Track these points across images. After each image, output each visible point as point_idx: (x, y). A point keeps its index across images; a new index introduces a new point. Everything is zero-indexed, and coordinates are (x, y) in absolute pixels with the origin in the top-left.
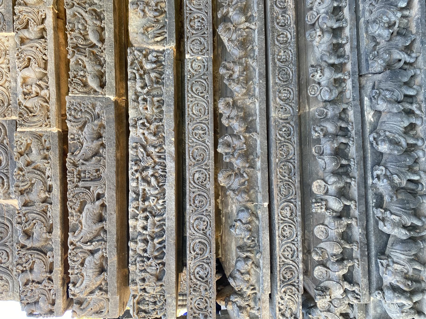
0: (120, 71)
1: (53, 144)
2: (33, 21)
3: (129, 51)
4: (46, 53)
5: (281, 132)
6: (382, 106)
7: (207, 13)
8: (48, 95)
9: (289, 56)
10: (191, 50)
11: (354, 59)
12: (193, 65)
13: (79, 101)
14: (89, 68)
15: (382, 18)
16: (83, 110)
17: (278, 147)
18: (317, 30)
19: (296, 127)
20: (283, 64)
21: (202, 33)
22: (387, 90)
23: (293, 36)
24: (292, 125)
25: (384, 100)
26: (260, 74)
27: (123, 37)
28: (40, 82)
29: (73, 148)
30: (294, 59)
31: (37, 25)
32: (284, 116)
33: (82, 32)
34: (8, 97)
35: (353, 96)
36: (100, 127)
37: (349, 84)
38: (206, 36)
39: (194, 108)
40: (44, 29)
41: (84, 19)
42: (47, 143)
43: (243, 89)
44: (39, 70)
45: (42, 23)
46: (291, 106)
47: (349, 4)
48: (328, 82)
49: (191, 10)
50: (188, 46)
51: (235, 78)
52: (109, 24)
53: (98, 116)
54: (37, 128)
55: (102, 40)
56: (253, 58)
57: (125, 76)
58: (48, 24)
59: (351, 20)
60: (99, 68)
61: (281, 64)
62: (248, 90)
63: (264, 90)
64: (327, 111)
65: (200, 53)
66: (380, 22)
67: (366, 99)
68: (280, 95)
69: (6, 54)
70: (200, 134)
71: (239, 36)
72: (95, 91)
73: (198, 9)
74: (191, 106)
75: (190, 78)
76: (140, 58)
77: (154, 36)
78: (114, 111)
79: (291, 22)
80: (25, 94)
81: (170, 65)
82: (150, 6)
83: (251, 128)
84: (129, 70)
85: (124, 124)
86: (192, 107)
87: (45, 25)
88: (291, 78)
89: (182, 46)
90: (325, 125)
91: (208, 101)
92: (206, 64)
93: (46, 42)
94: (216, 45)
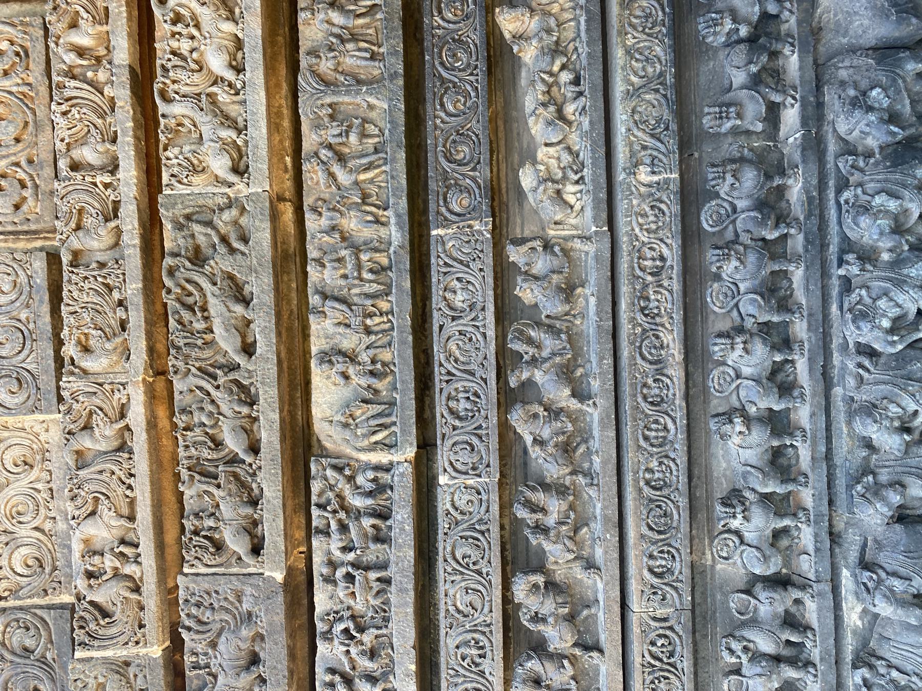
0: (293, 492)
1: (151, 684)
2: (102, 415)
4: (133, 485)
5: (654, 649)
6: (884, 609)
7: (485, 381)
8: (139, 574)
9: (671, 473)
10: (451, 463)
11: (820, 484)
12: (456, 498)
13: (206, 586)
14: (227, 511)
15: (886, 409)
16: (216, 605)
17: (648, 682)
18: (736, 420)
19: (687, 637)
20: (658, 493)
22: (895, 574)
23: (681, 427)
24: (677, 633)
25: (888, 598)
26: (606, 519)
27: (300, 413)
28: (122, 549)
29: (195, 682)
30: (683, 479)
31: (112, 422)
32: (661, 612)
33: (210, 431)
35: (817, 571)
36: (253, 640)
37: (806, 536)
38: (484, 432)
39: (458, 596)
40: (128, 428)
41: (213, 402)
42: (140, 680)
43: (567, 554)
44: (119, 523)
45: (123, 416)
46: (676, 589)
47: (809, 359)
48: (760, 536)
49: (449, 373)
50: (443, 456)
51: (548, 525)
52: (269, 413)
53: (250, 614)
54: (118, 649)
55: (254, 449)
56: (587, 474)
57: (303, 499)
59: (814, 395)
60: (249, 511)
61: (653, 492)
62: (580, 545)
63: (616, 555)
64: (757, 602)
65: (470, 472)
66: (881, 419)
67: (845, 573)
68: (651, 563)
69: (44, 460)
70: (472, 656)
71: (557, 434)
72: (240, 558)
73: (465, 371)
74: (451, 592)
75: (449, 528)
76: (340, 486)
77: (369, 431)
78: (283, 607)
79: (674, 395)
80: (90, 575)
81: (405, 501)
82: (360, 364)
83: (587, 631)
84: (315, 512)
85: (304, 609)
86: (454, 596)
87: (127, 420)
88: (675, 525)
89: (427, 407)
90: (752, 638)
91: (490, 582)
92: (484, 497)
93: (130, 458)
94: (502, 400)
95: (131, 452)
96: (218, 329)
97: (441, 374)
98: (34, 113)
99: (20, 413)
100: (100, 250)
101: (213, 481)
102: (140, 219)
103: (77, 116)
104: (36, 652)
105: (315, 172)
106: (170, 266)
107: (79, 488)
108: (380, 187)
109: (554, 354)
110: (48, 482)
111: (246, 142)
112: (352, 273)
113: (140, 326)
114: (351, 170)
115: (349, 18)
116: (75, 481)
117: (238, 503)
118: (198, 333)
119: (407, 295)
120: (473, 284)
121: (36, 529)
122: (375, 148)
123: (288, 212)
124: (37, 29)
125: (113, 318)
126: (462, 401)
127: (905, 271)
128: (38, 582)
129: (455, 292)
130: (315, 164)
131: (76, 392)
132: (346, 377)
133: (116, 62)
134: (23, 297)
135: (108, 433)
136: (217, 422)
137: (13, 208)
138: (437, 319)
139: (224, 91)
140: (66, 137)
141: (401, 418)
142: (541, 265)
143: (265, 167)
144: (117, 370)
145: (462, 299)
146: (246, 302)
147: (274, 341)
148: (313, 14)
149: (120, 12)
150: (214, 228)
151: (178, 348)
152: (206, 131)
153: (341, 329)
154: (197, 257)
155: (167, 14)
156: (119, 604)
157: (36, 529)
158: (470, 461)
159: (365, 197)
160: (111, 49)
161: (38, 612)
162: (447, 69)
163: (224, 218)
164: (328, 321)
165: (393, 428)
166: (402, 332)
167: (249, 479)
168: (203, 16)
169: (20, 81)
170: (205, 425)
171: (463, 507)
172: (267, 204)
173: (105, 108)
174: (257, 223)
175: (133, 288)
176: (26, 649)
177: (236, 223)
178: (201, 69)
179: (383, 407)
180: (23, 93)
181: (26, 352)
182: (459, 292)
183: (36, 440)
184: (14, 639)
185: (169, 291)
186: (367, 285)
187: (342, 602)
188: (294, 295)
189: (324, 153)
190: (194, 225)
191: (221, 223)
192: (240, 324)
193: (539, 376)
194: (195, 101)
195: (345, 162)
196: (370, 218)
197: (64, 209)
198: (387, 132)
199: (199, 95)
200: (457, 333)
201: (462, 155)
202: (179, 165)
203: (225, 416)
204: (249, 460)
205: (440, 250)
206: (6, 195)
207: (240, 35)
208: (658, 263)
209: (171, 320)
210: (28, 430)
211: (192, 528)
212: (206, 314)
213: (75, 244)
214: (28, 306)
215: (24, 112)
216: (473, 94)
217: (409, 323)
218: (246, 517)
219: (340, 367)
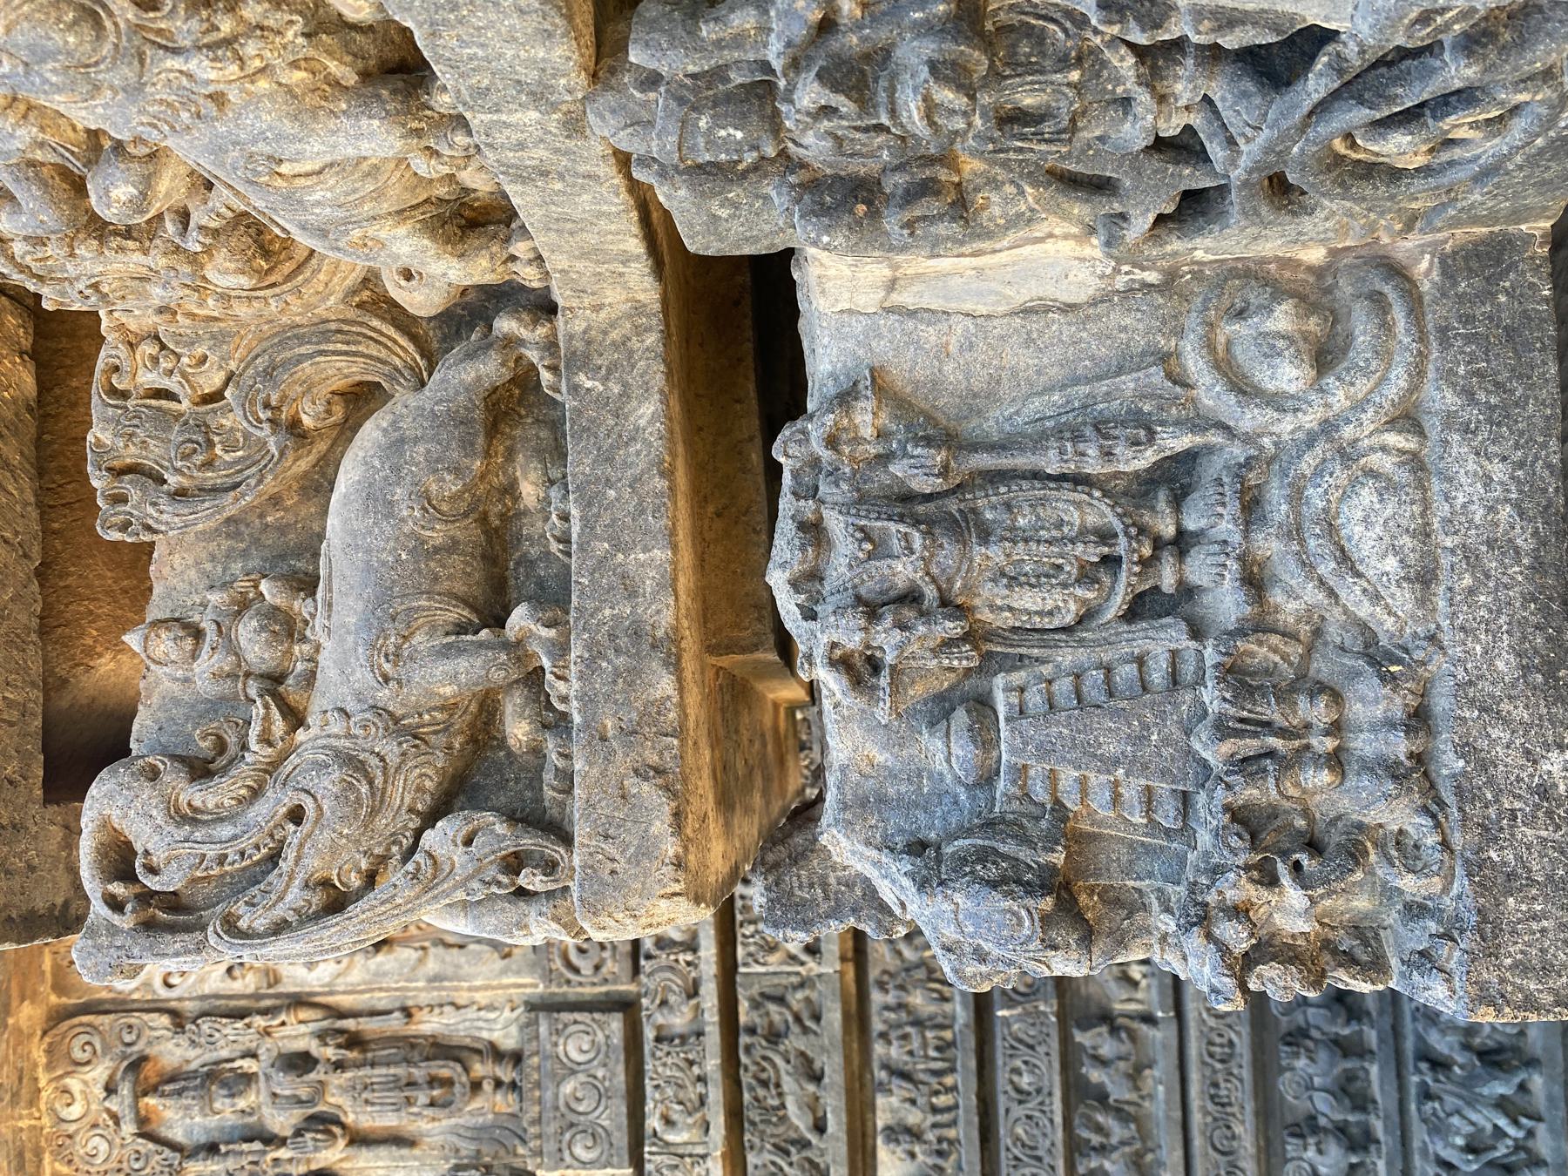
49: (1016, 1158)
96: (792, 1108)
109: (1123, 1143)
125: (693, 1092)
127: (1477, 1090)
132: (912, 1155)
134: (601, 1056)
138: (1002, 1102)
142: (1107, 1048)
146: (817, 1078)
151: (753, 1123)
153: (907, 1105)
175: (712, 1064)
177: (808, 1000)
181: (601, 1109)
193: (1107, 1165)
196: (935, 995)
208: (1227, 1050)
213: (660, 1019)
214: (605, 1065)
219: (907, 1146)
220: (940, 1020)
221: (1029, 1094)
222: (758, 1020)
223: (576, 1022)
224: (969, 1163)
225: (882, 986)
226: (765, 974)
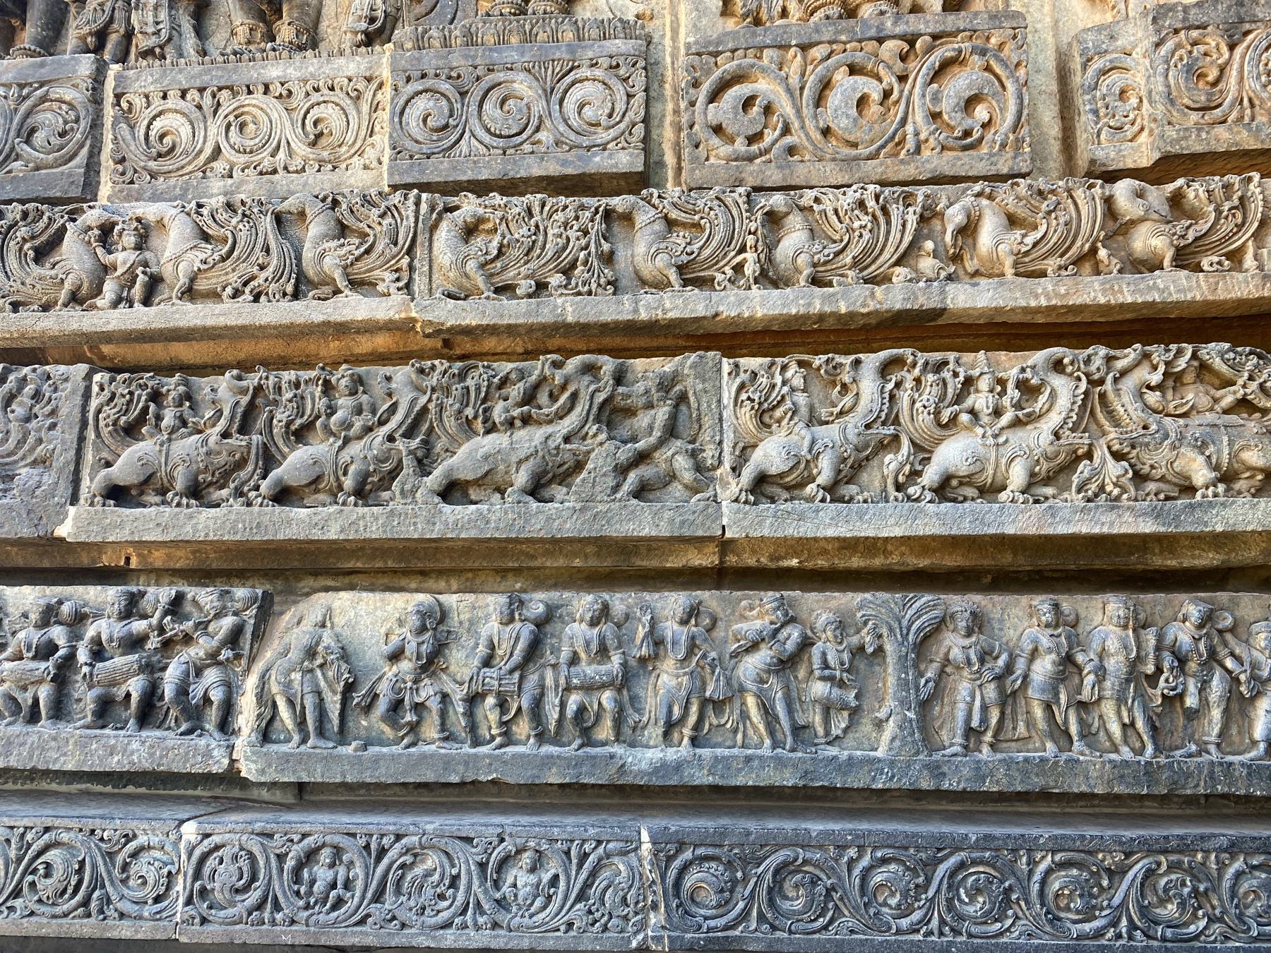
2: (357, 253)
3: (241, 592)
4: (240, 299)
7: (362, 922)
10: (217, 848)
13: (64, 411)
16: (33, 424)
21: (281, 900)
28: (141, 279)
31: (345, 267)
33: (318, 423)
34: (178, 169)
40: (337, 292)
41: (370, 429)
45: (357, 284)
49: (382, 852)
52: (340, 522)
55: (283, 495)
57: (214, 566)
58: (344, 306)
60: (179, 485)
65: (197, 885)
75: (102, 839)
81: (161, 757)
82: (416, 682)
87: (347, 292)
93: (285, 294)
95: (296, 296)
97: (382, 836)
98: (871, 157)
99: (394, 129)
100: (633, 256)
101: (236, 427)
102: (682, 321)
103: (856, 224)
104: (25, 147)
105: (760, 616)
106: (601, 368)
107: (244, 215)
108: (735, 731)
110: (285, 168)
111: (810, 500)
112: (577, 676)
113: (502, 316)
114: (762, 681)
115: (1043, 691)
116: (255, 210)
117: (194, 467)
118: (485, 411)
119: (535, 776)
120: (544, 908)
121: (217, 151)
122: (804, 727)
123: (706, 559)
124: (1010, 163)
125: (520, 275)
126: (329, 875)
128: (135, 151)
129: (533, 870)
130: (773, 617)
131: (399, 213)
132: (395, 656)
133: (951, 288)
134: (573, 136)
135: (328, 262)
136: (335, 435)
137: (715, 123)
139: (902, 465)
140: (822, 207)
141: (309, 755)
143: (766, 532)
144: (434, 277)
145: (519, 884)
146: (536, 489)
147: (463, 536)
148: (1047, 626)
149: (1037, 296)
150: (662, 442)
151: (462, 376)
152: (829, 434)
153: (482, 650)
154: (616, 410)
155: (1035, 373)
156: (53, 272)
157: (217, 151)
158: (217, 885)
159: (718, 705)
160: (976, 280)
161: (85, 151)
162: (953, 874)
163: (679, 458)
164: (496, 625)
165: (296, 738)
166: (466, 763)
167: (232, 486)
168: (1035, 433)
169: (923, 137)
170: (329, 416)
171: (133, 870)
172: (700, 533)
173: (873, 267)
174: (667, 515)
176: (33, 131)
177: (672, 477)
178: (945, 427)
179: (336, 722)
180: (903, 141)
181: (487, 138)
182: (532, 879)
183: (352, 151)
184: (49, 115)
185: (557, 365)
186: (557, 701)
187: (14, 634)
188: (561, 562)
189: (793, 635)
190: (667, 409)
191: (670, 453)
192: (498, 478)
194: (883, 415)
195: (777, 672)
196: (677, 712)
197: (700, 203)
198: (833, 751)
199: (896, 421)
200: (454, 872)
201: (792, 894)
202: (773, 386)
203: (341, 448)
204: (264, 485)
205: (611, 846)
206: (736, 114)
207: (1003, 496)
209: (510, 366)
210: (369, 140)
211: (164, 390)
212: (518, 423)
215: (872, 142)
216: (904, 923)
217: (483, 778)
218: (171, 478)
219: (411, 648)
220: (632, 718)
221: (497, 885)
222: (640, 387)
223: (630, 96)
224: (377, 760)
225: (692, 613)
226: (719, 401)
